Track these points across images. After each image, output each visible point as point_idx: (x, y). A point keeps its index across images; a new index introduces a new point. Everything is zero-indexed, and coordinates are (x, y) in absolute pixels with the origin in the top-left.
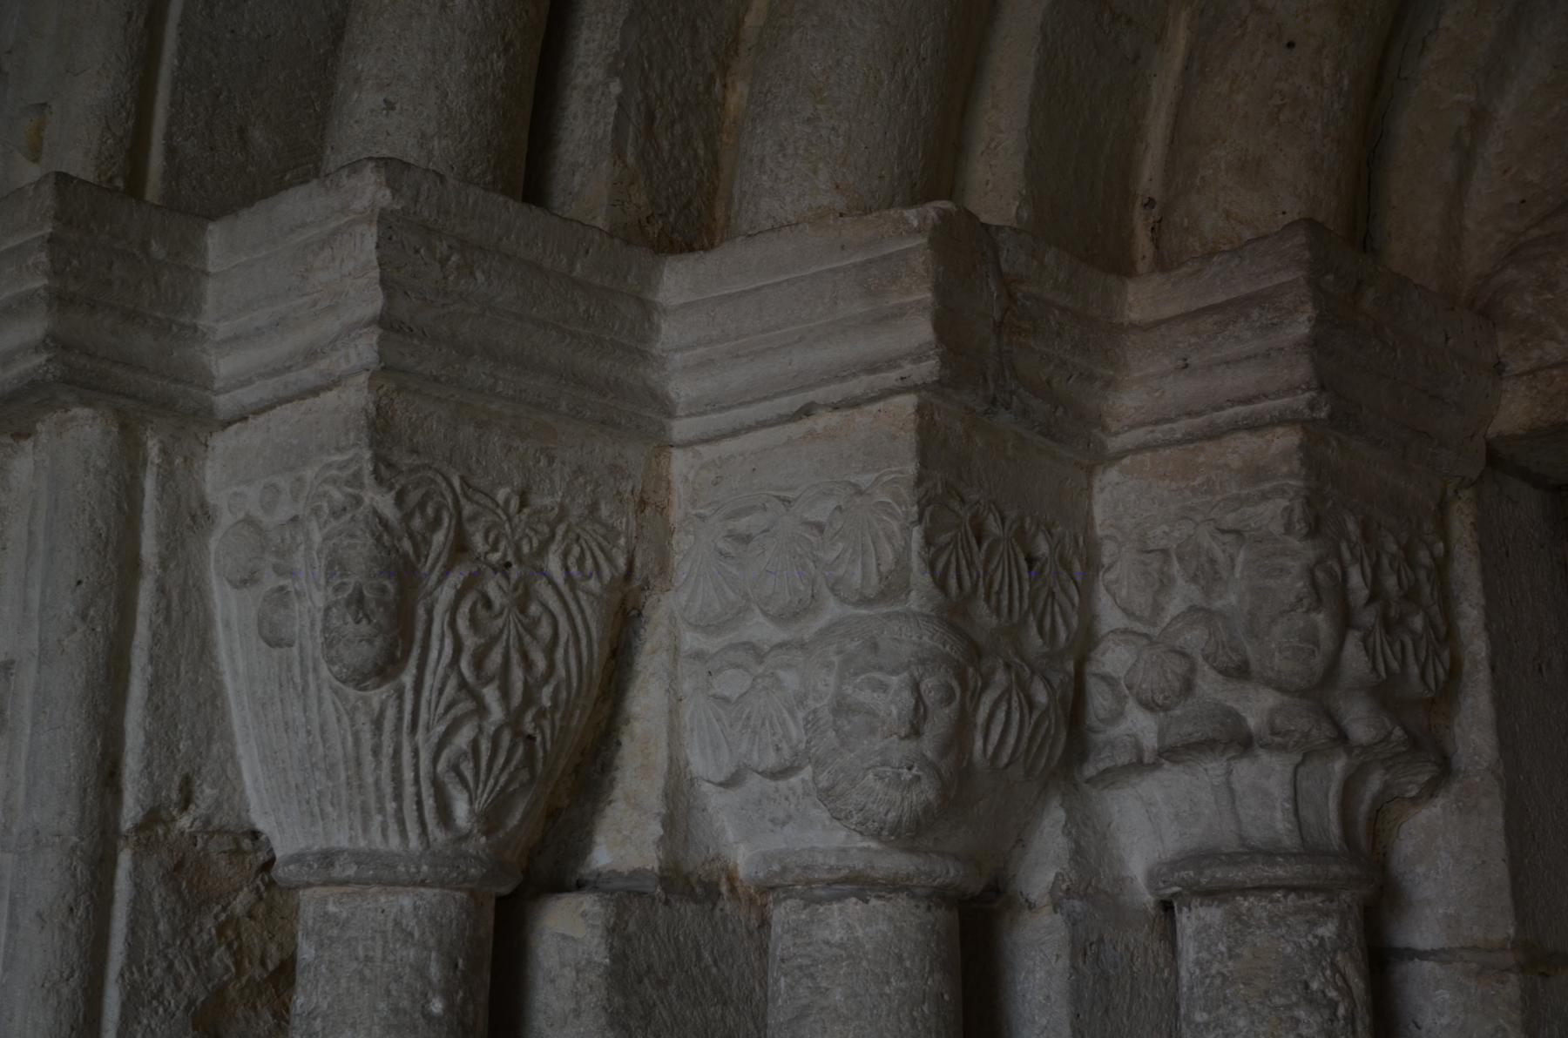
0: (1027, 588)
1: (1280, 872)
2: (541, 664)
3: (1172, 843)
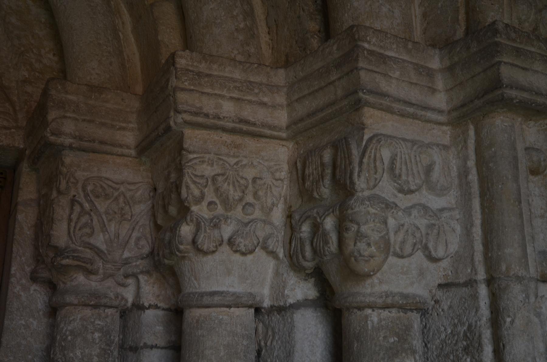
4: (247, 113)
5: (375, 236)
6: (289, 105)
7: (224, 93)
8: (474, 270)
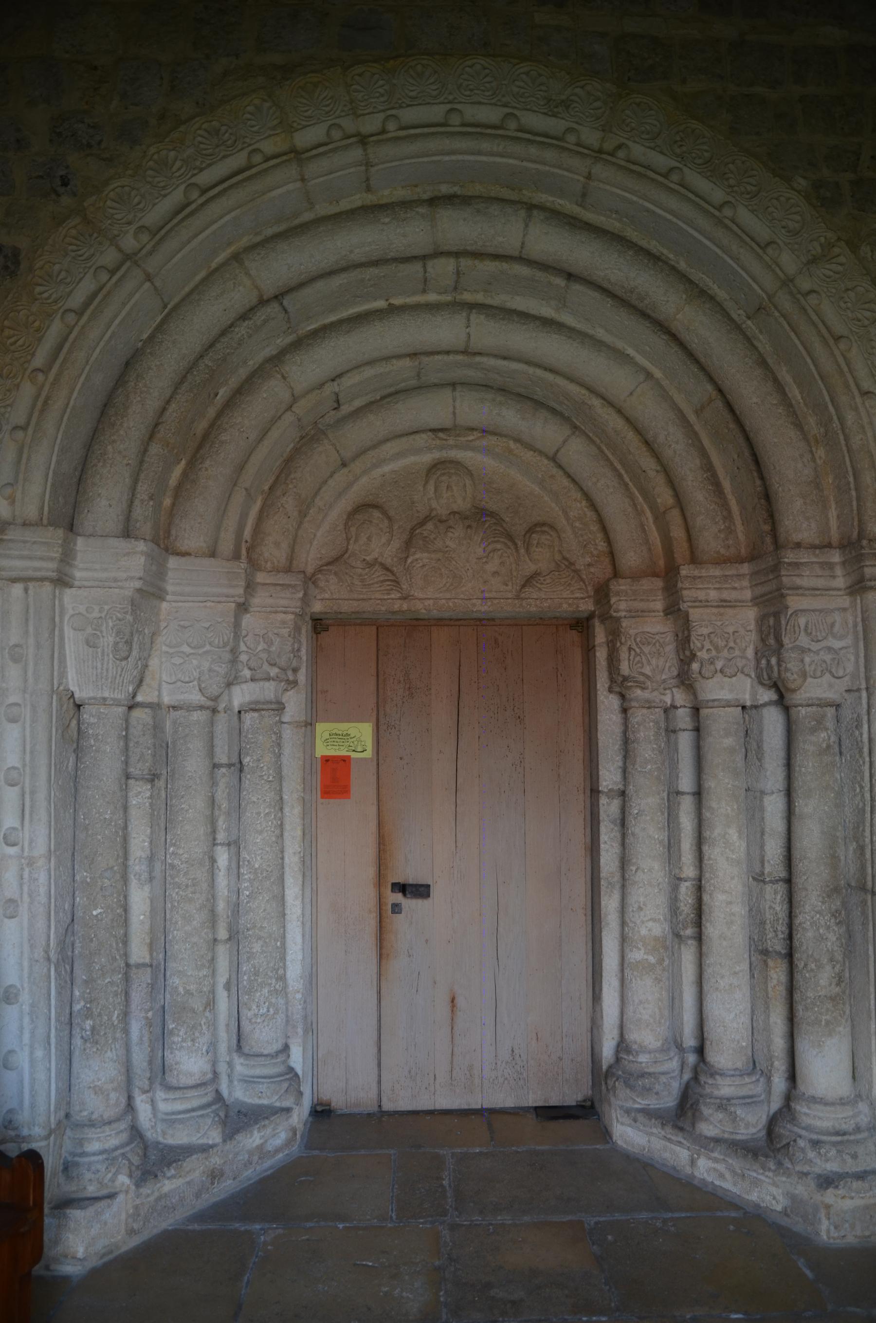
3: (247, 699)
4: (725, 595)
5: (795, 669)
6: (751, 587)
7: (710, 586)
8: (860, 684)
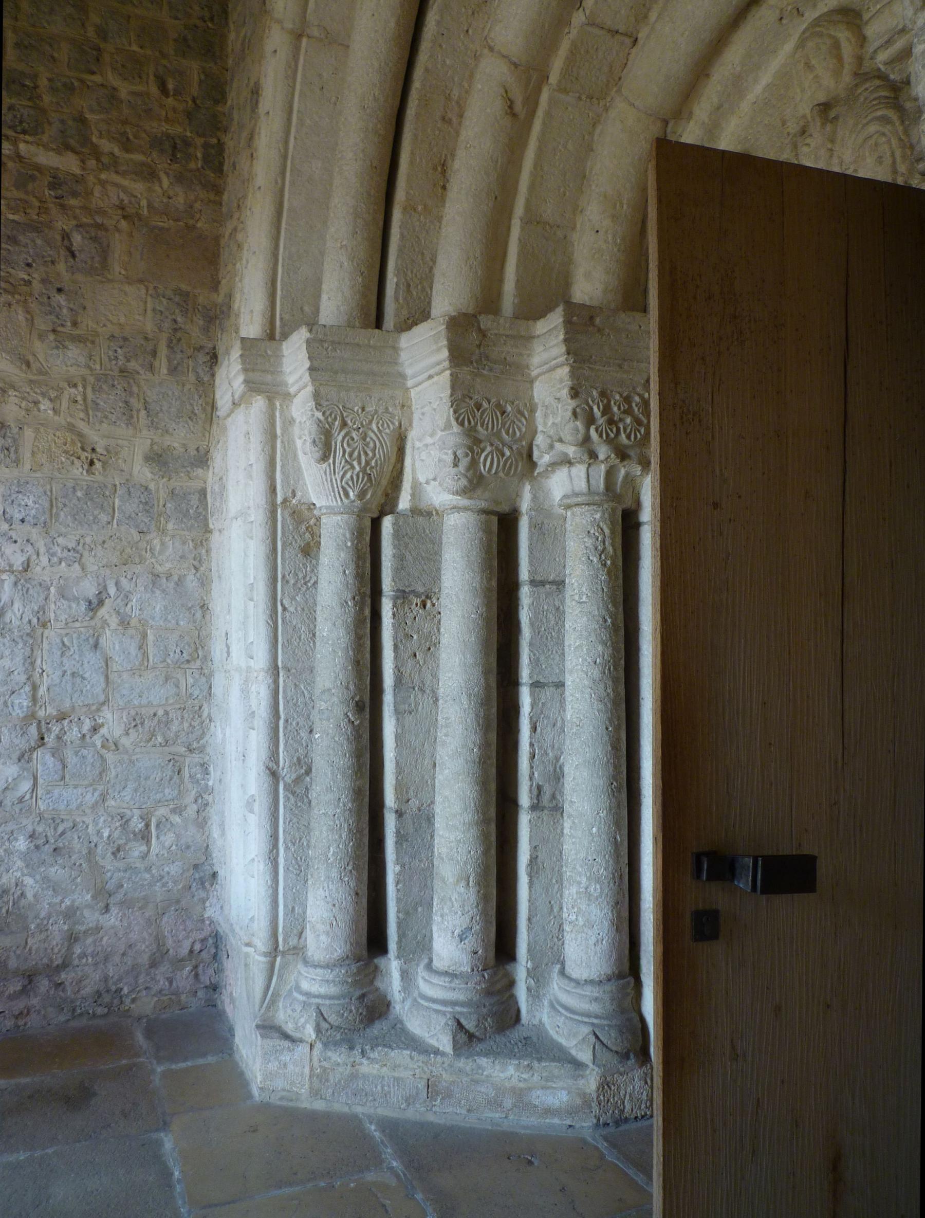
0: (500, 421)
1: (579, 499)
2: (371, 454)
